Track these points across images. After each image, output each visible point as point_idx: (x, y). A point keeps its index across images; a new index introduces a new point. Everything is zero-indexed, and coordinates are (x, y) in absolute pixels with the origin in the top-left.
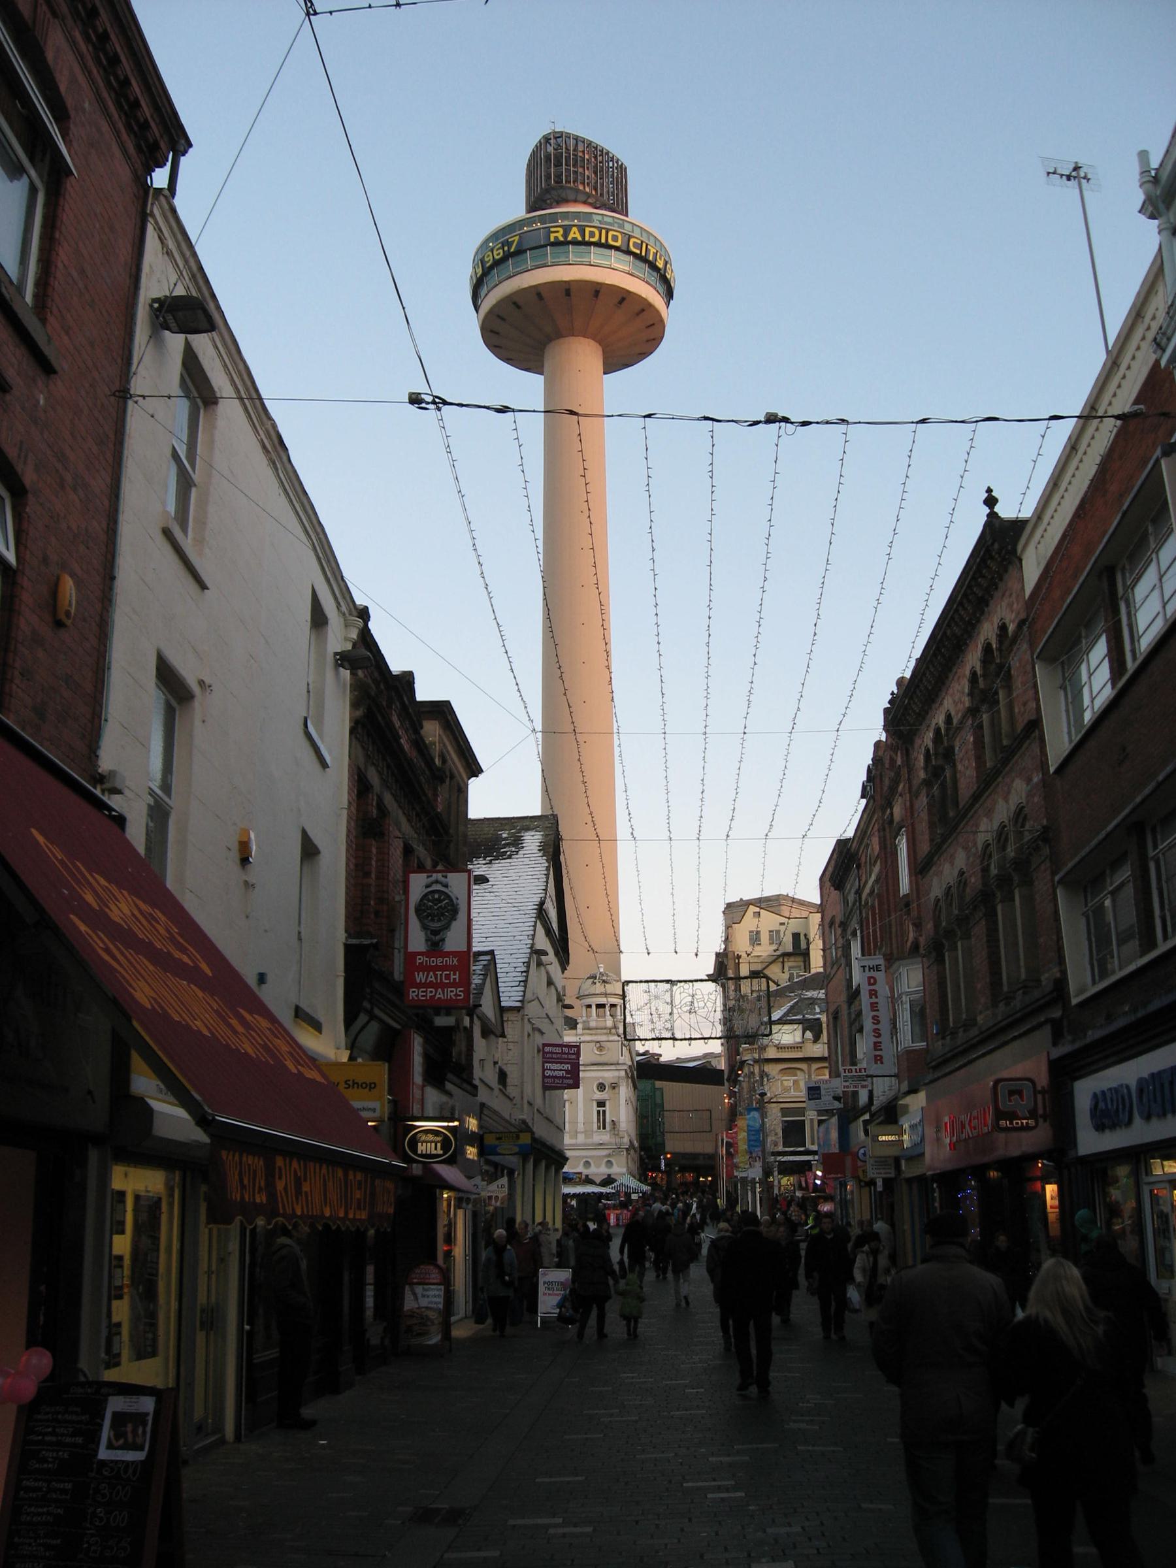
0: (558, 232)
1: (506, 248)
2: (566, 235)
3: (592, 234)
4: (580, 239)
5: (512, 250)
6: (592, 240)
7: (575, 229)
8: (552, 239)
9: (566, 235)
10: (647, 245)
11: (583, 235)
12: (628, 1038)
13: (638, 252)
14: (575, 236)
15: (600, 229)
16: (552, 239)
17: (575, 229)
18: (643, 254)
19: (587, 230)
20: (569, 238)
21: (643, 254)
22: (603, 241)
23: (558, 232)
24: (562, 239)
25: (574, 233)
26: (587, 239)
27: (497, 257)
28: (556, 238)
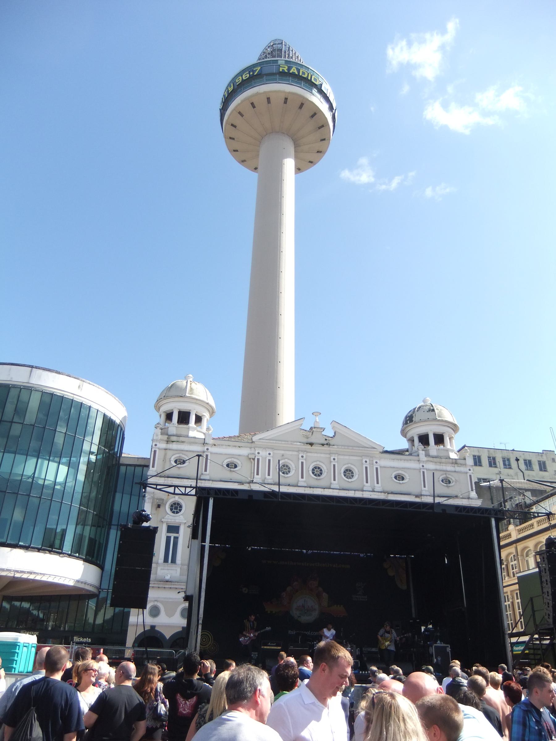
0: (285, 67)
2: (289, 68)
4: (297, 73)
5: (255, 74)
6: (303, 76)
7: (294, 68)
8: (281, 70)
9: (289, 68)
14: (294, 71)
16: (281, 70)
20: (291, 72)
23: (285, 67)
24: (286, 71)
25: (294, 70)
26: (301, 74)
27: (244, 78)
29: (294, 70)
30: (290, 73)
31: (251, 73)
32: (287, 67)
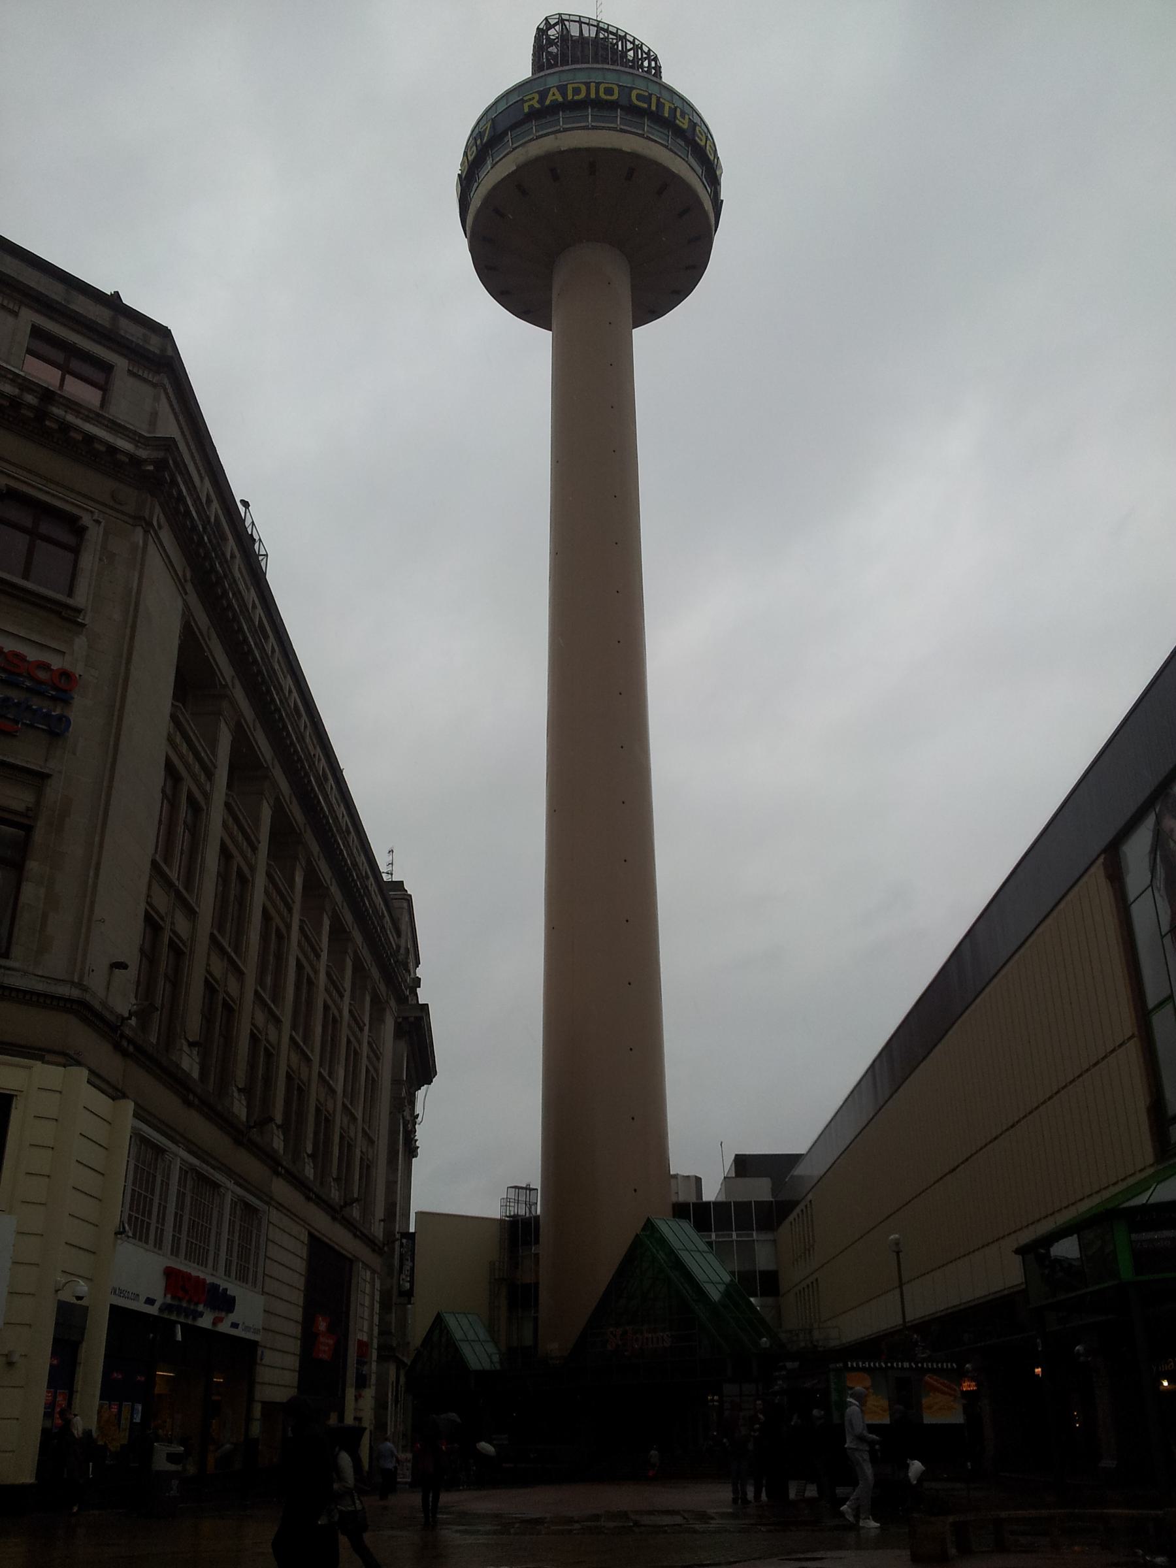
1: (479, 142)
3: (577, 91)
4: (560, 99)
6: (576, 98)
10: (658, 99)
11: (564, 95)
12: (266, 1290)
13: (645, 106)
14: (554, 98)
15: (587, 85)
17: (554, 90)
18: (654, 108)
19: (570, 87)
20: (548, 102)
21: (654, 108)
22: (593, 96)
24: (537, 106)
25: (554, 95)
26: (570, 98)
28: (531, 107)
29: (554, 95)
30: (548, 107)
31: (479, 142)
32: (537, 97)
